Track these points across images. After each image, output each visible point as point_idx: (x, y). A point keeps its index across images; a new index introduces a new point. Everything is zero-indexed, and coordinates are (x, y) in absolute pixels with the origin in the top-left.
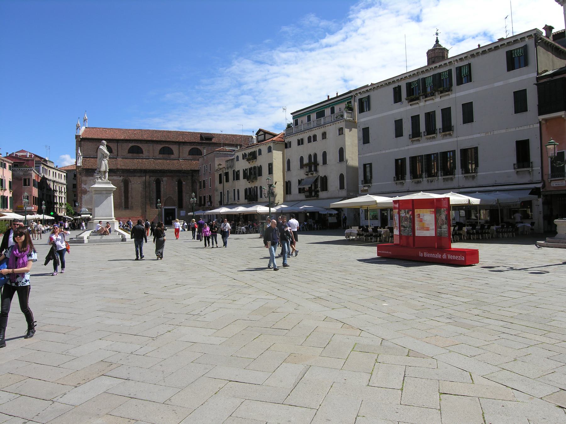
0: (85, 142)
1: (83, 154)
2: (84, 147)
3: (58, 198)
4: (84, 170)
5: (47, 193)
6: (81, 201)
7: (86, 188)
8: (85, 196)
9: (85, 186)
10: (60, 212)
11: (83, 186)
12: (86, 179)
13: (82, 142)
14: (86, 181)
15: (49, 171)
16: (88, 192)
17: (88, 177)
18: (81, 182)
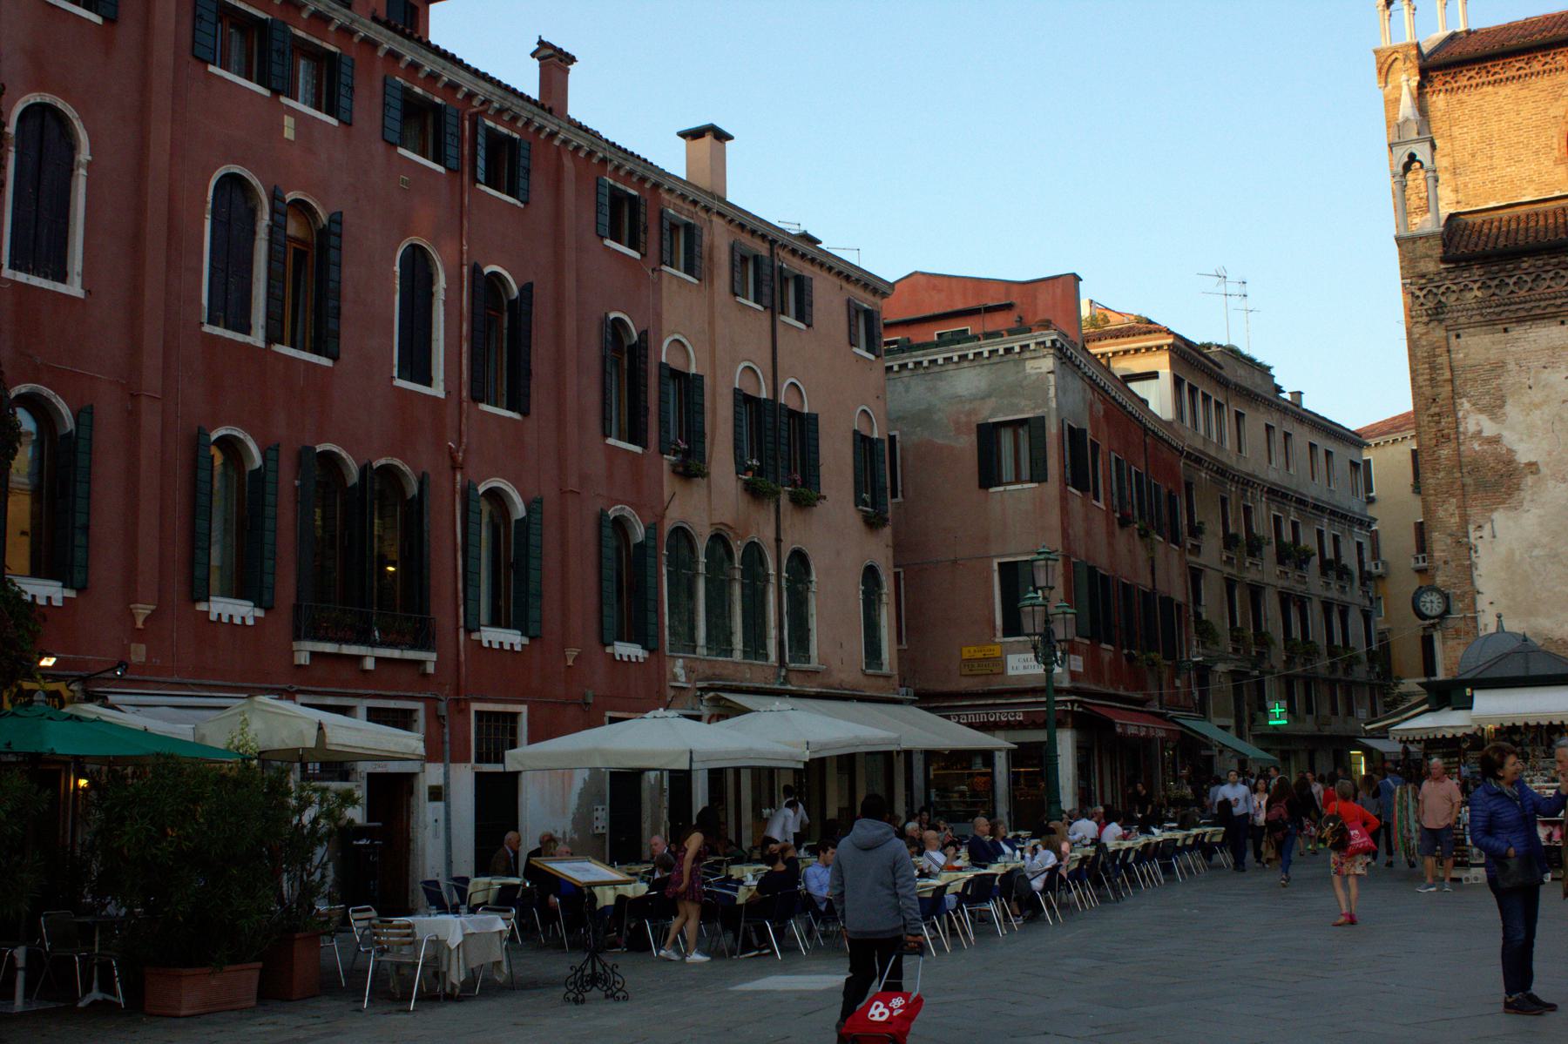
0: (1461, 95)
1: (1456, 191)
2: (1456, 131)
3: (1315, 612)
4: (1468, 268)
5: (1227, 570)
6: (1469, 570)
7: (1510, 439)
8: (1499, 516)
9: (1489, 428)
10: (1334, 711)
11: (1474, 422)
12: (1494, 354)
13: (1438, 102)
14: (1499, 367)
15: (1239, 416)
16: (1530, 480)
17: (1517, 332)
18: (1452, 381)
